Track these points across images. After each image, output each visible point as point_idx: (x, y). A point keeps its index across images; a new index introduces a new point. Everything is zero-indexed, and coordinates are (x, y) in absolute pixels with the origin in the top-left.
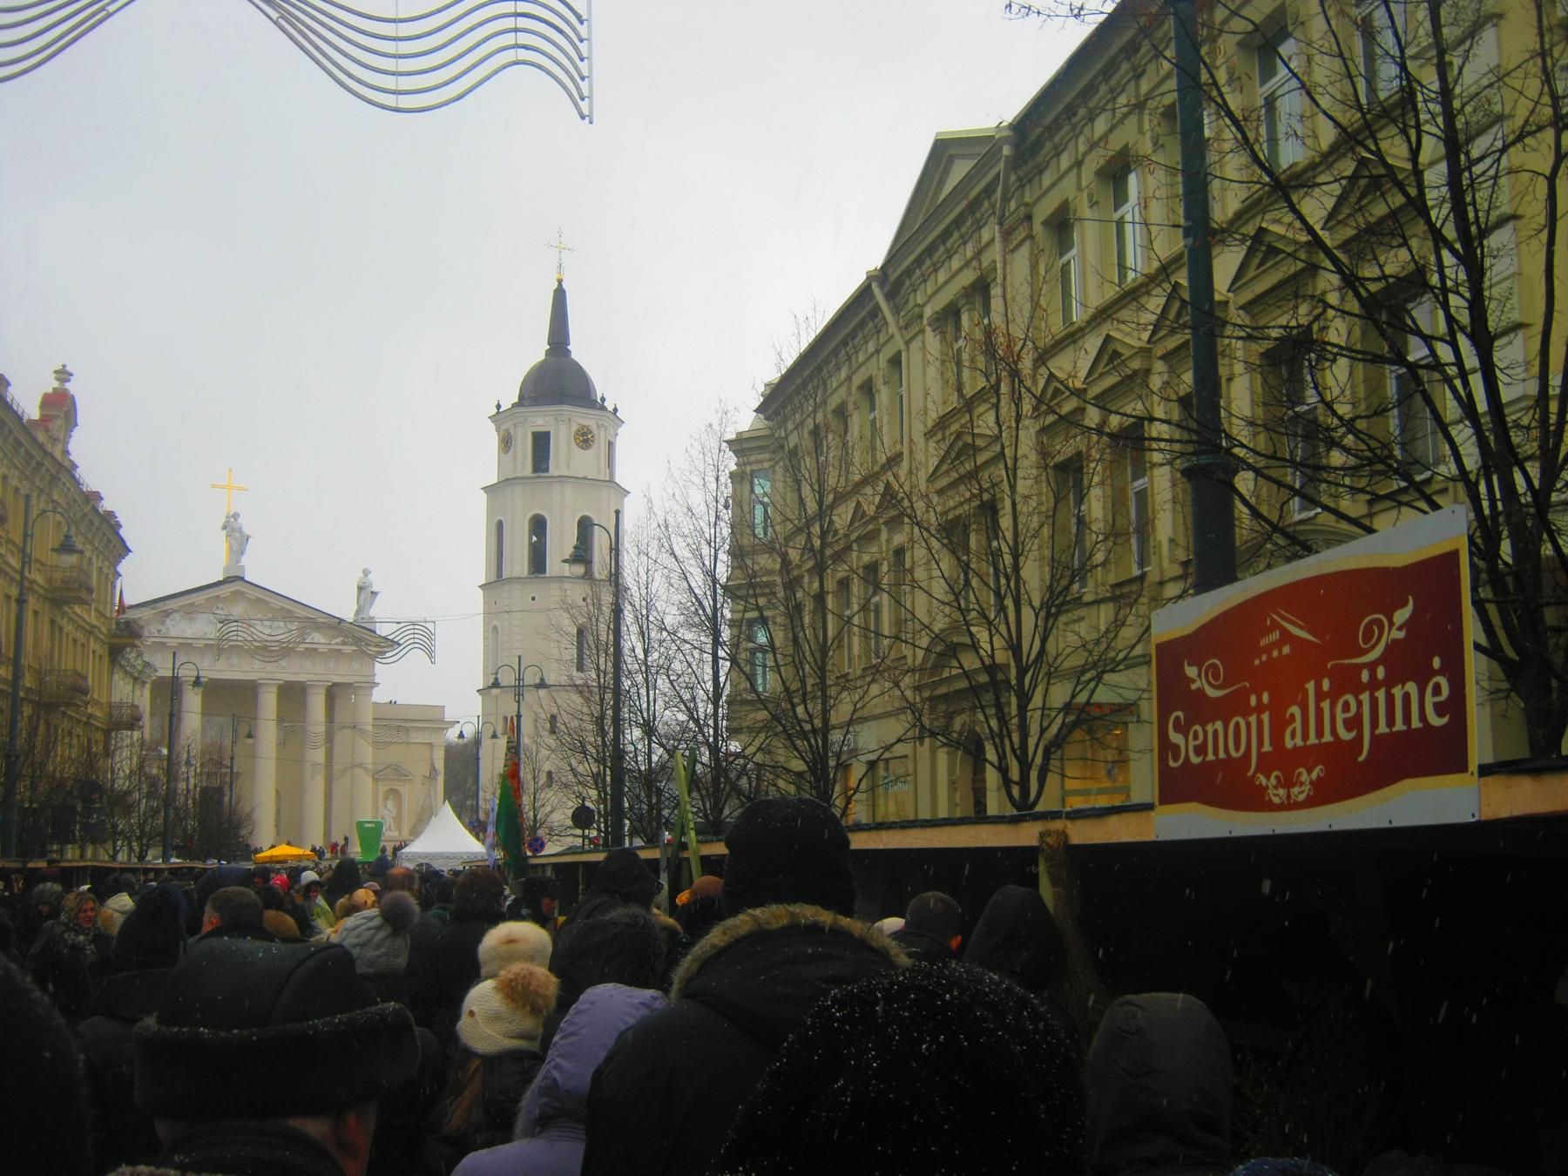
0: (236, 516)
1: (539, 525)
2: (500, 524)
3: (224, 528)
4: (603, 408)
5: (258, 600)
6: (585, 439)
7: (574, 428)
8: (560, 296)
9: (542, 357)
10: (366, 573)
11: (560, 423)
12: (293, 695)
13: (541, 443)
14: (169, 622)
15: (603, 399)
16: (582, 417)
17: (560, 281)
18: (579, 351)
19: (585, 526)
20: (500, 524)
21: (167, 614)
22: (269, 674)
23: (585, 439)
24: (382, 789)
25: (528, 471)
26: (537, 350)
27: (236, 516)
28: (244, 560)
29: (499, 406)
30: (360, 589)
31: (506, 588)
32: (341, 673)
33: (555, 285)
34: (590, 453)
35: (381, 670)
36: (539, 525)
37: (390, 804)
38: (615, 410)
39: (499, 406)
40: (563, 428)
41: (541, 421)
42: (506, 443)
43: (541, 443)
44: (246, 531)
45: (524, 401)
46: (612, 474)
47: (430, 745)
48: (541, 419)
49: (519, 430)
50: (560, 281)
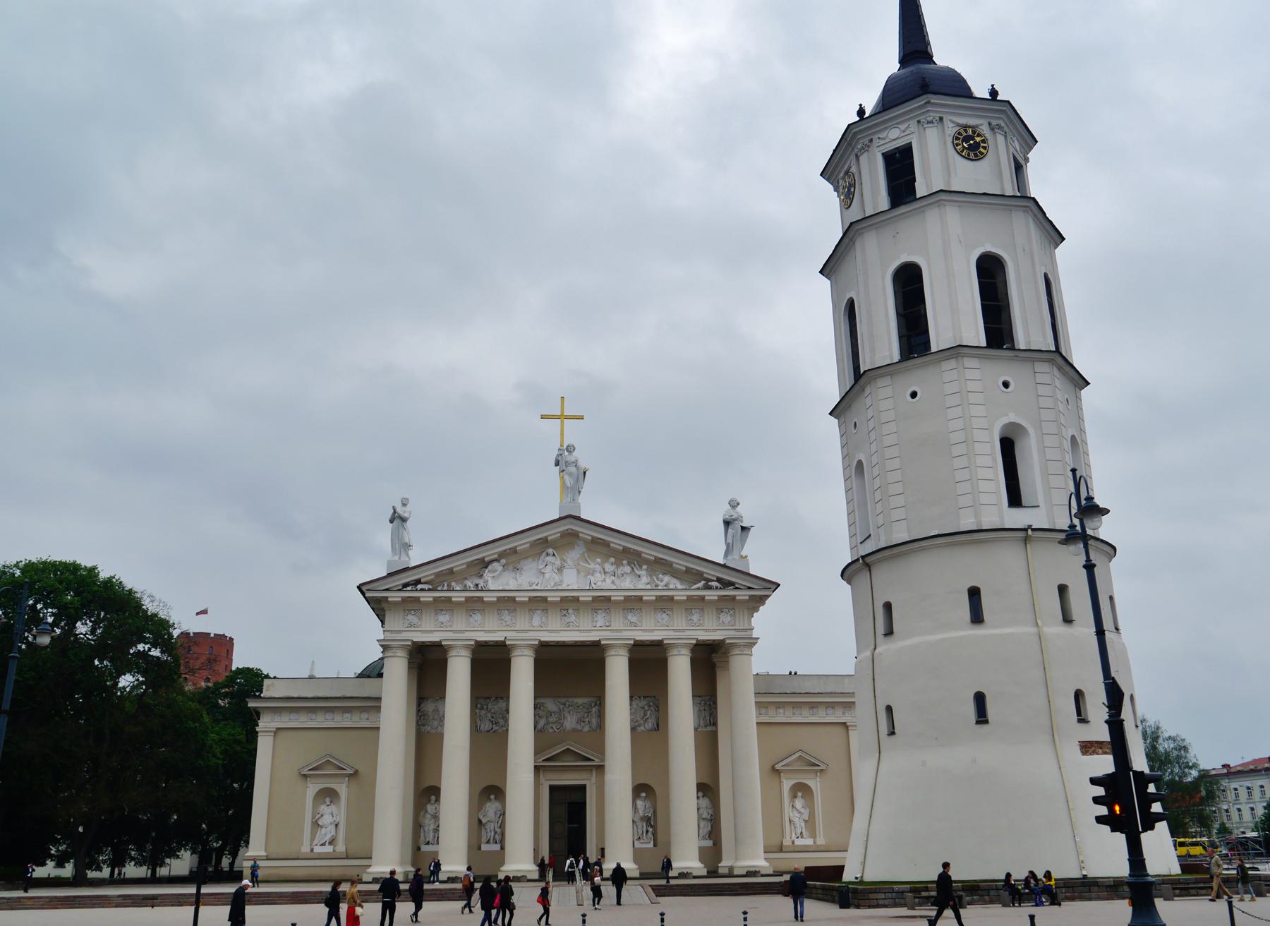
0: (570, 449)
1: (909, 283)
3: (557, 464)
5: (595, 541)
6: (971, 146)
7: (951, 130)
10: (734, 504)
12: (648, 663)
13: (900, 167)
14: (487, 575)
15: (994, 93)
16: (957, 118)
18: (944, 55)
20: (851, 306)
21: (484, 564)
22: (617, 632)
24: (787, 784)
27: (570, 449)
28: (582, 499)
30: (727, 523)
32: (710, 629)
35: (763, 621)
36: (909, 283)
37: (799, 803)
40: (932, 133)
41: (894, 133)
44: (582, 465)
47: (844, 724)
49: (864, 159)
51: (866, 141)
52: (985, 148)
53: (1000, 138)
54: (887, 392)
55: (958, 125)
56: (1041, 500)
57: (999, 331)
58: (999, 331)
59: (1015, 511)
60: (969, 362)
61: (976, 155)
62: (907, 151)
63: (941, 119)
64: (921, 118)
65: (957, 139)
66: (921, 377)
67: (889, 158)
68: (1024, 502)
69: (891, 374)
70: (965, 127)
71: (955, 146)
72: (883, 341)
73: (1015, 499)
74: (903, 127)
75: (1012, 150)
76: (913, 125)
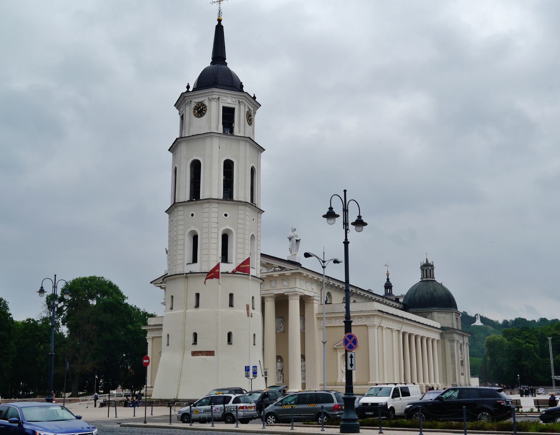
8: (219, 30)
15: (254, 98)
23: (250, 119)
25: (221, 130)
26: (206, 61)
29: (188, 87)
33: (217, 23)
34: (251, 127)
39: (188, 87)
40: (242, 107)
41: (229, 100)
51: (217, 97)
54: (216, 210)
55: (248, 108)
60: (248, 209)
62: (233, 110)
64: (240, 100)
66: (227, 208)
67: (224, 109)
69: (218, 203)
72: (212, 185)
74: (234, 100)
76: (237, 103)
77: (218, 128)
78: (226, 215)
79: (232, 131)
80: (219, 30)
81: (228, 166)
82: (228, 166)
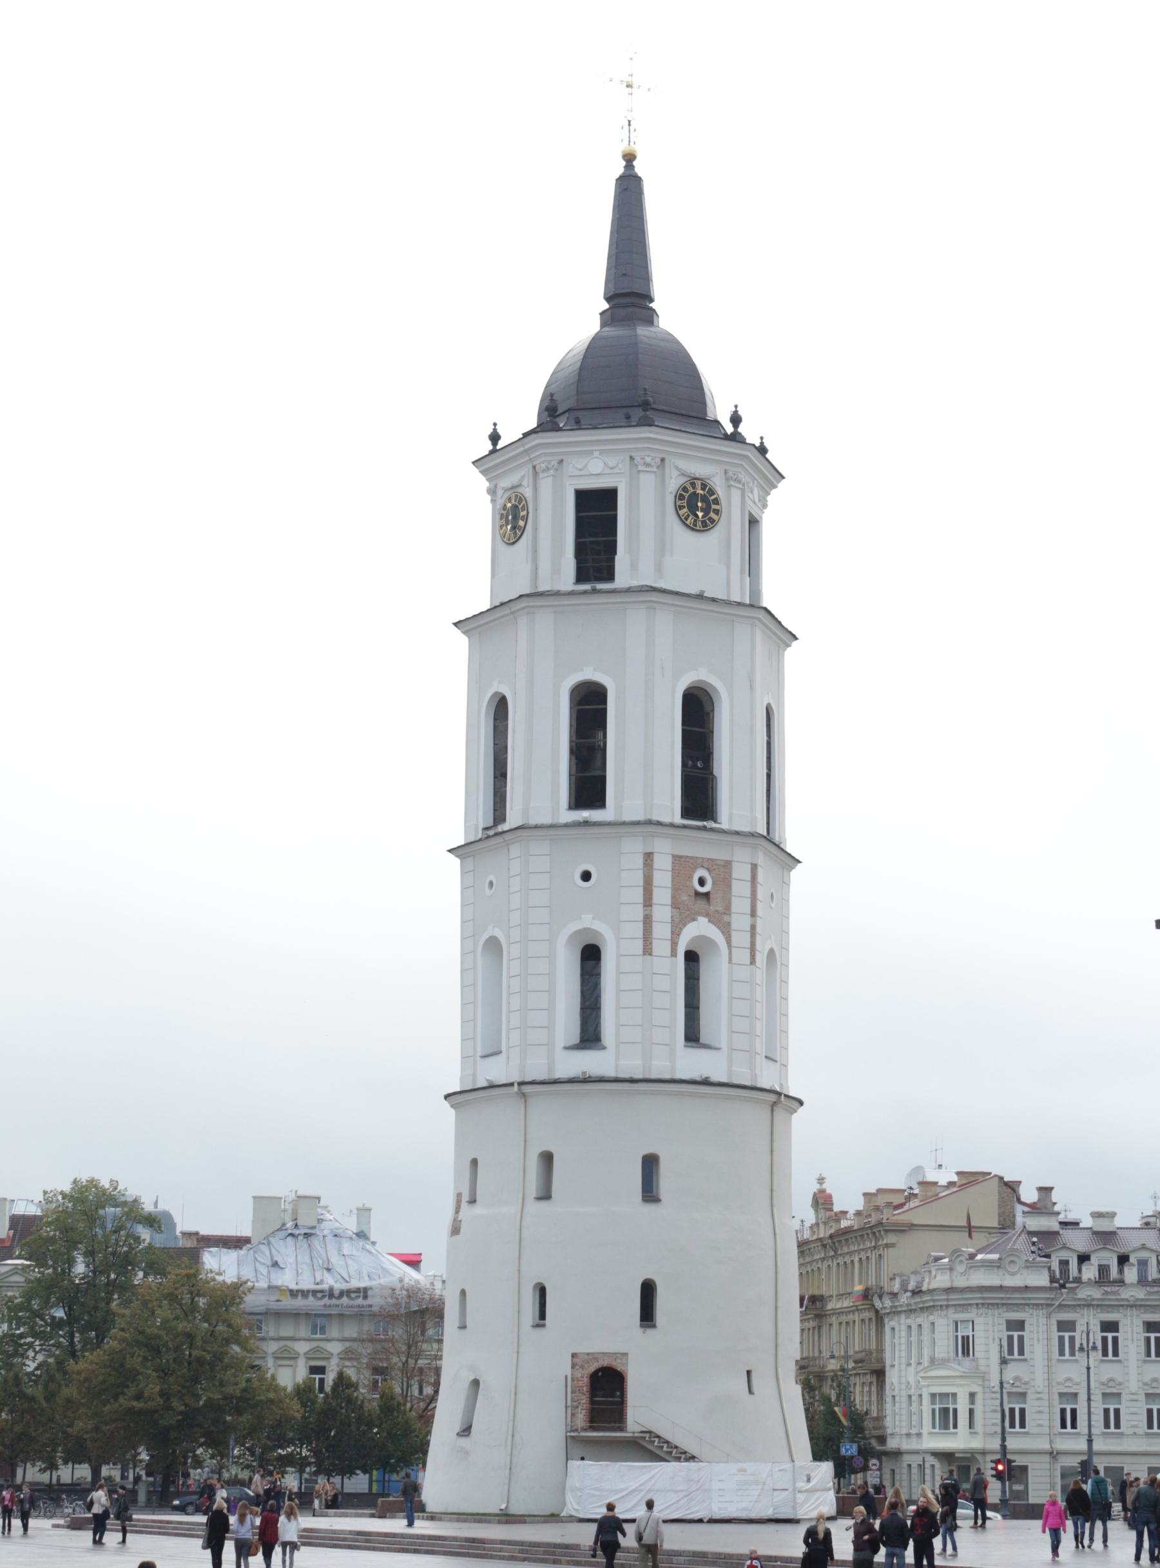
2: (500, 708)
4: (736, 438)
6: (697, 506)
7: (674, 483)
8: (629, 189)
9: (593, 326)
11: (638, 469)
13: (596, 513)
15: (736, 420)
17: (629, 158)
19: (697, 709)
20: (500, 708)
23: (697, 506)
29: (495, 437)
31: (515, 850)
33: (619, 168)
34: (713, 537)
38: (762, 450)
39: (495, 437)
40: (648, 482)
42: (513, 519)
43: (596, 513)
45: (553, 415)
46: (756, 592)
48: (596, 460)
49: (546, 484)
50: (629, 158)
52: (717, 512)
53: (736, 495)
56: (723, 1043)
57: (699, 796)
58: (699, 796)
59: (696, 1054)
61: (704, 524)
63: (663, 460)
65: (681, 497)
68: (702, 1041)
70: (693, 481)
71: (678, 508)
73: (692, 1036)
74: (612, 462)
75: (748, 508)
76: (624, 467)
77: (556, 571)
78: (586, 876)
79: (608, 574)
80: (629, 189)
81: (589, 708)
82: (589, 708)
